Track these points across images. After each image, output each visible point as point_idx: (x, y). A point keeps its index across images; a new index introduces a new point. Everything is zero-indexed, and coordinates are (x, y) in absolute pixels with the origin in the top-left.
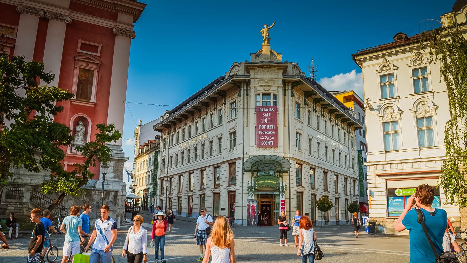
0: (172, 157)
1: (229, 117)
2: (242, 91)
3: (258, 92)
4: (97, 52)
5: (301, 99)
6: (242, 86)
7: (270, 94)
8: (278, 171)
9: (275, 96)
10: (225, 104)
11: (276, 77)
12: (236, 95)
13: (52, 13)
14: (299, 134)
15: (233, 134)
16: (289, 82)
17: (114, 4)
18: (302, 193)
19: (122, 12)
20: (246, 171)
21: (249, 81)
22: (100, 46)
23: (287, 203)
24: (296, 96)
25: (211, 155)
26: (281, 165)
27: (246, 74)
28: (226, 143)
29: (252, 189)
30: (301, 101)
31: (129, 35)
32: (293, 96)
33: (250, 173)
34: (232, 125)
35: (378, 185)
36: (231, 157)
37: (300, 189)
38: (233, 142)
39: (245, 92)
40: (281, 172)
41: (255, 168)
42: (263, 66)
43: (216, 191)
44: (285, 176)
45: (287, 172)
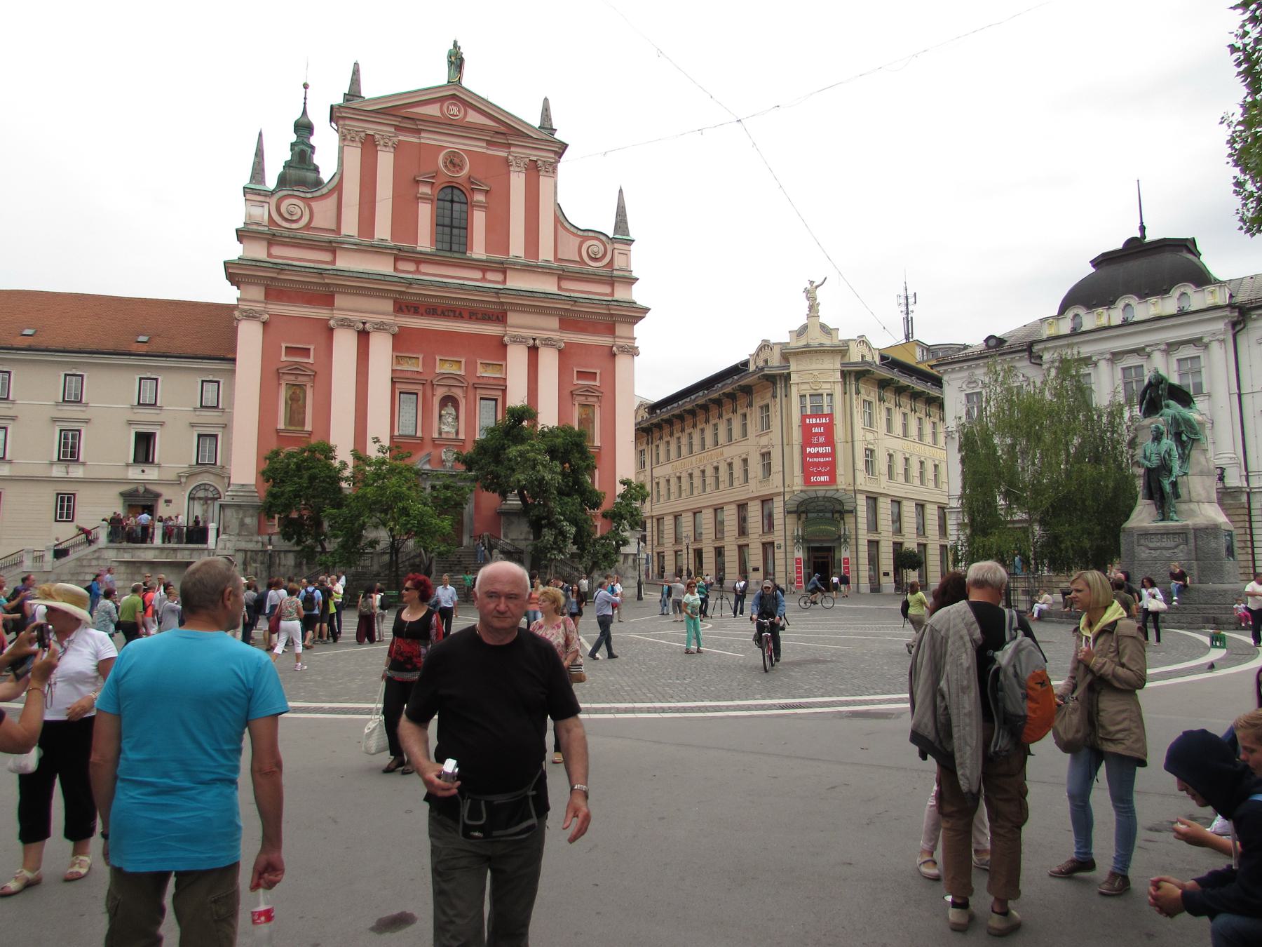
0: (658, 484)
1: (759, 427)
3: (803, 393)
4: (595, 380)
5: (872, 394)
9: (830, 395)
10: (750, 405)
12: (769, 395)
13: (542, 340)
15: (766, 455)
16: (850, 372)
17: (612, 315)
18: (877, 542)
19: (621, 322)
20: (789, 512)
21: (789, 374)
23: (854, 556)
24: (863, 391)
25: (731, 484)
26: (841, 503)
28: (755, 467)
30: (873, 397)
31: (633, 352)
32: (858, 392)
33: (795, 516)
34: (764, 440)
36: (765, 491)
37: (874, 537)
38: (768, 468)
40: (842, 513)
41: (802, 509)
42: (810, 352)
43: (742, 541)
44: (849, 519)
45: (851, 512)
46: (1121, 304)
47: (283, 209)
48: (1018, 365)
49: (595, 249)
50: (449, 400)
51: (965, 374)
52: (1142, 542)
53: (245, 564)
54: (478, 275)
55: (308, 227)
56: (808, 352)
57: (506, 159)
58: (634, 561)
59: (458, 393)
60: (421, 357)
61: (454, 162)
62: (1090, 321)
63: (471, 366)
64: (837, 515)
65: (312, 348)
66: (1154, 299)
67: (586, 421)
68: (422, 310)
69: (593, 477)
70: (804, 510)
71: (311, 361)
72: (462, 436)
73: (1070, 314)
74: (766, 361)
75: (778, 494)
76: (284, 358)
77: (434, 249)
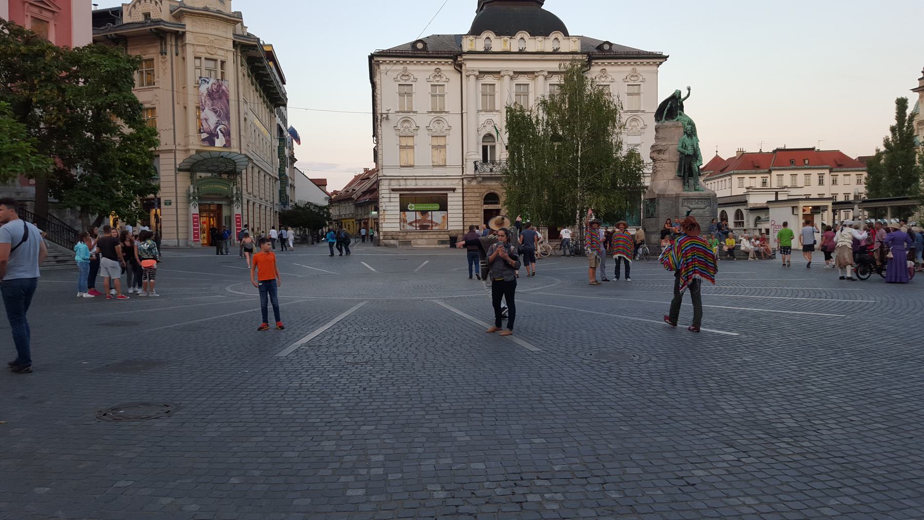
2: (169, 47)
3: (199, 55)
6: (168, 39)
7: (216, 60)
8: (225, 173)
9: (223, 63)
11: (224, 35)
14: (245, 119)
20: (180, 170)
21: (184, 33)
27: (173, 21)
29: (189, 198)
33: (188, 174)
35: (392, 200)
39: (174, 48)
42: (207, 16)
46: (519, 36)
48: (442, 67)
51: (400, 67)
52: (686, 204)
56: (205, 15)
62: (498, 44)
64: (225, 176)
66: (540, 38)
70: (191, 168)
73: (484, 35)
74: (147, 15)
75: (170, 151)
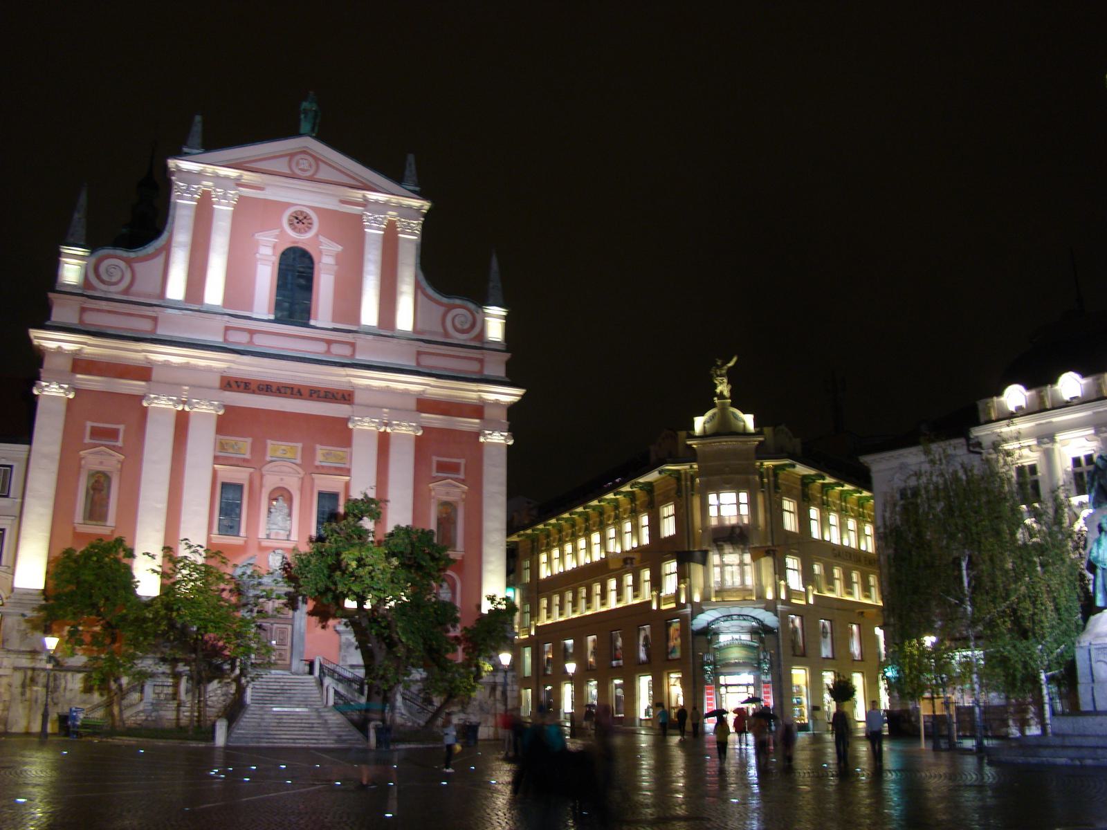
22: (462, 461)
47: (102, 269)
49: (463, 319)
50: (281, 494)
53: (23, 686)
54: (322, 347)
55: (126, 291)
57: (359, 218)
58: (504, 693)
59: (292, 483)
60: (249, 440)
61: (300, 220)
63: (308, 453)
65: (121, 427)
67: (446, 521)
68: (253, 387)
69: (453, 588)
71: (120, 444)
72: (294, 537)
76: (87, 440)
77: (272, 317)
